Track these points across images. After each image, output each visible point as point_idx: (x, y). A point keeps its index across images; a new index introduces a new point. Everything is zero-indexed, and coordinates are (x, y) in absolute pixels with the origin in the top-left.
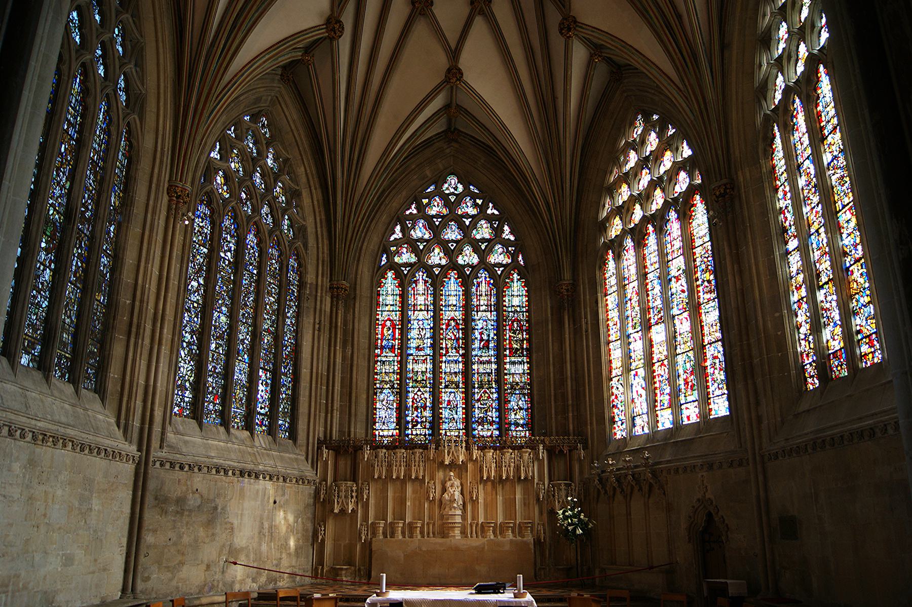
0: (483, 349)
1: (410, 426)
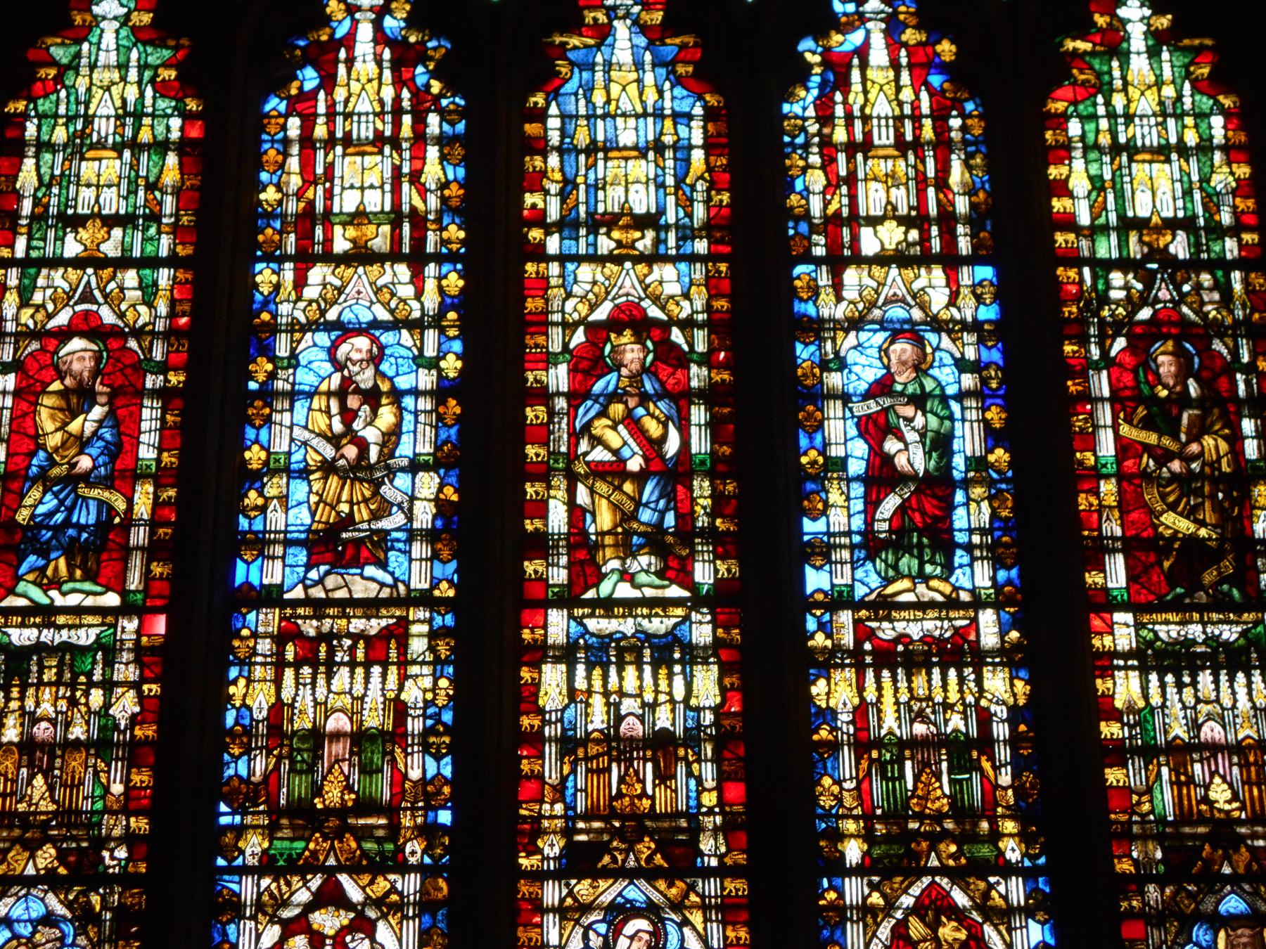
0: (899, 541)
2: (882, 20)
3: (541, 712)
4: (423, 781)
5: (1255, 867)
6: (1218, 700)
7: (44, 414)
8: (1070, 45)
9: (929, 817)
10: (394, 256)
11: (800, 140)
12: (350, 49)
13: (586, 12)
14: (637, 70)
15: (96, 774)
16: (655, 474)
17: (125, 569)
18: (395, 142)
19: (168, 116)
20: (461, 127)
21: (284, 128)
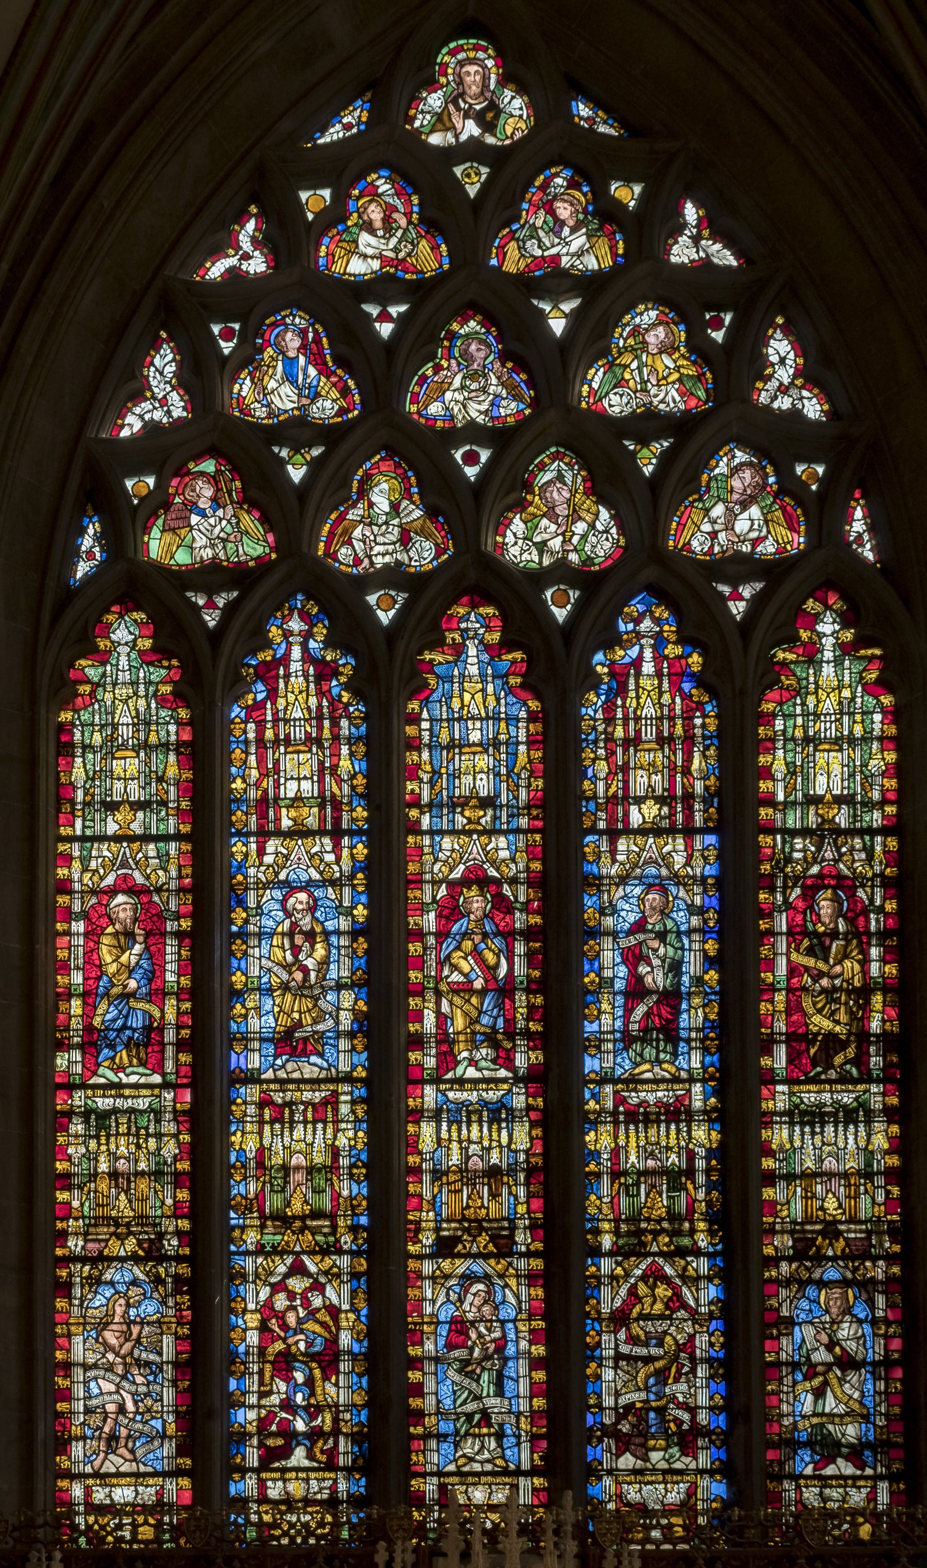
0: (644, 1037)
1: (253, 1457)
2: (651, 637)
3: (420, 1153)
4: (351, 1198)
5: (847, 1250)
6: (835, 1144)
7: (104, 949)
8: (781, 655)
9: (654, 1220)
10: (322, 832)
11: (591, 737)
12: (287, 667)
13: (447, 633)
14: (482, 682)
15: (156, 1192)
16: (492, 990)
17: (163, 1059)
18: (319, 742)
19: (168, 723)
20: (363, 729)
21: (245, 732)
